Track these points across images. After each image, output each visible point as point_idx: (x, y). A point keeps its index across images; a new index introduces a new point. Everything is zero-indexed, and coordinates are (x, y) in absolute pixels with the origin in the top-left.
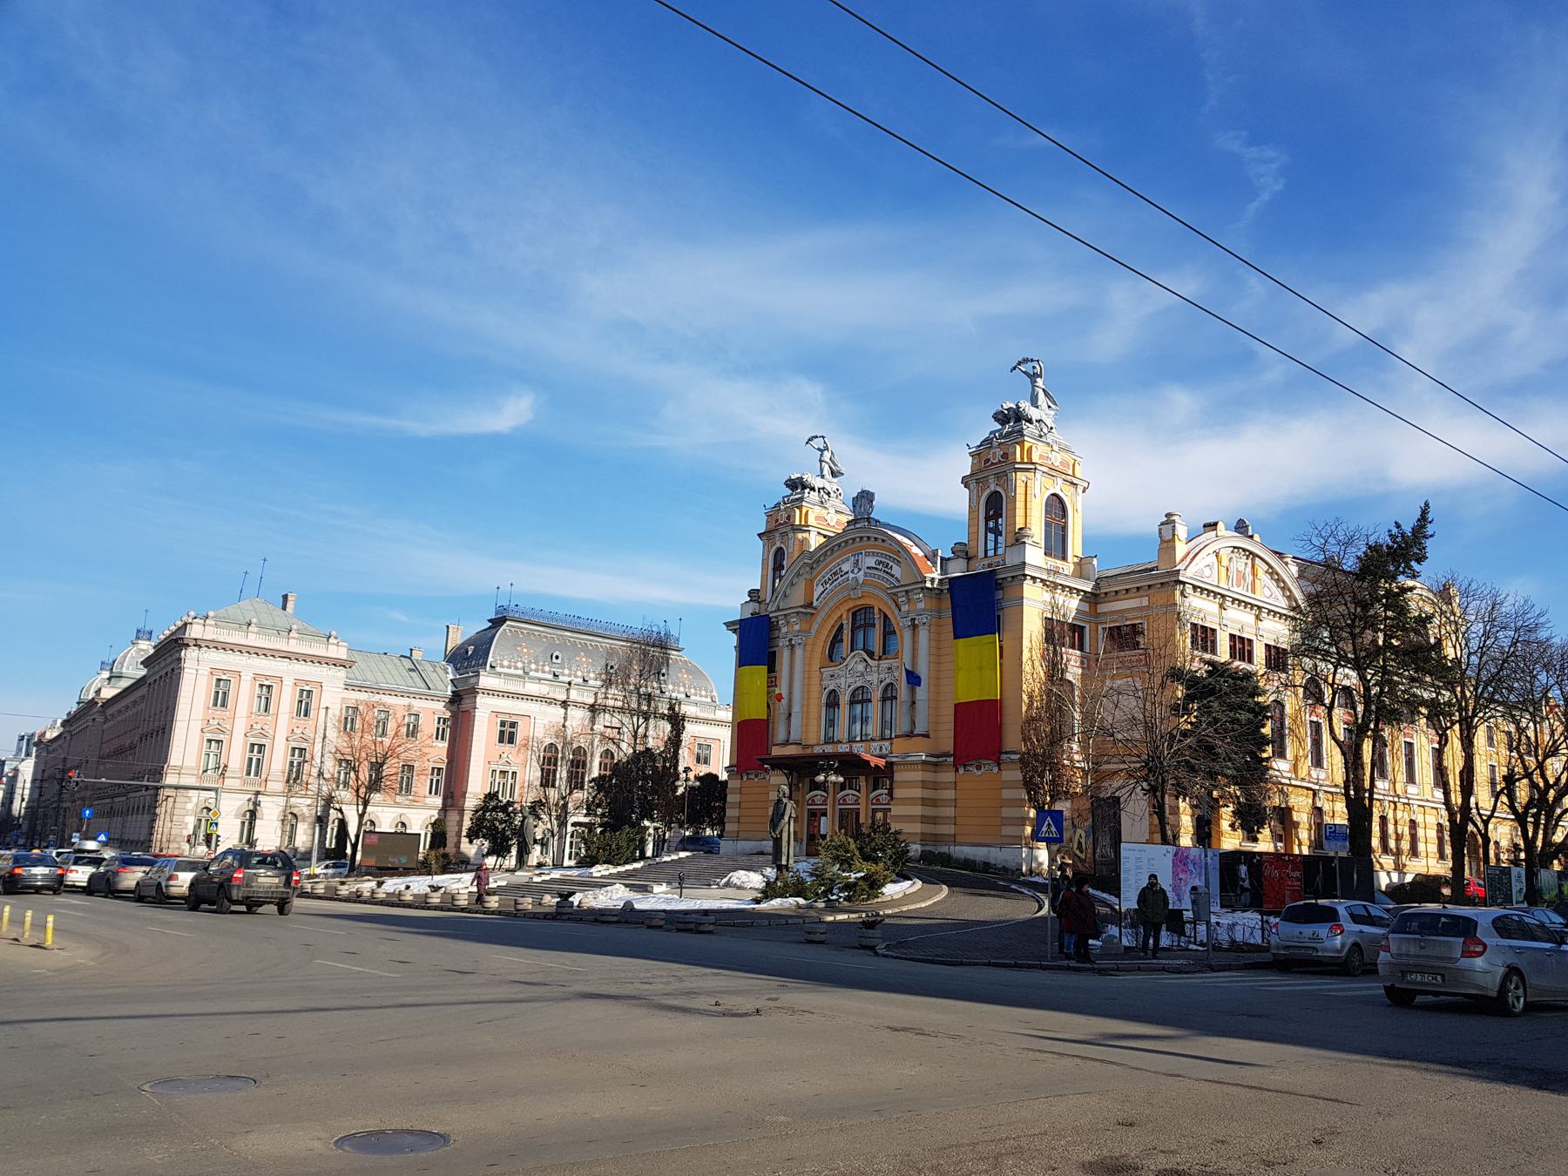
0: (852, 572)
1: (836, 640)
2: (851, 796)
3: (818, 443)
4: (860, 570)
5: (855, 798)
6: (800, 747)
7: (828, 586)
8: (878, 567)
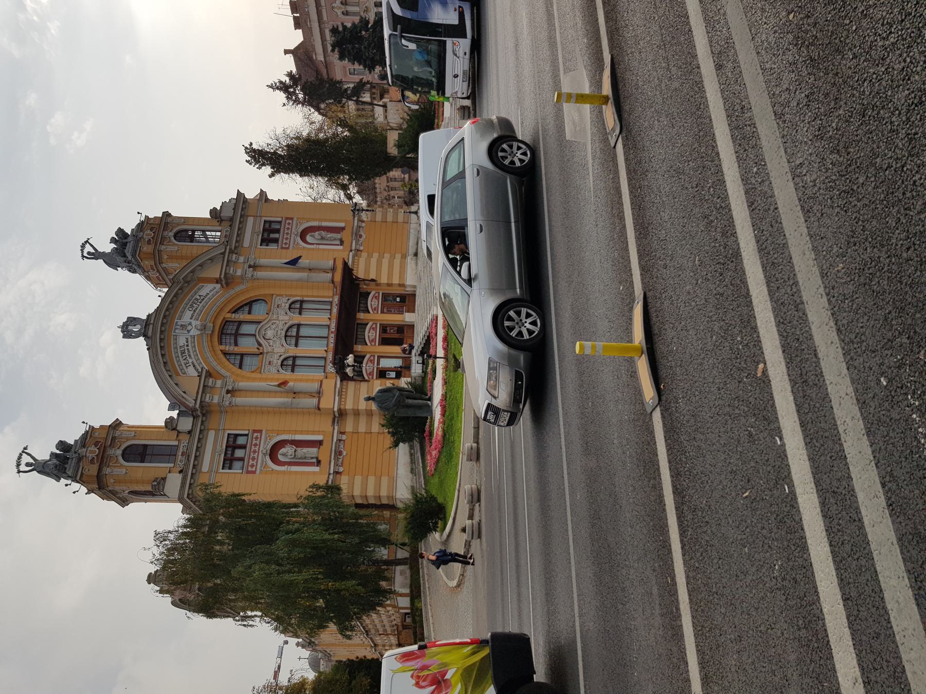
0: (189, 331)
2: (370, 334)
3: (23, 468)
4: (190, 324)
5: (372, 330)
7: (190, 361)
8: (194, 309)
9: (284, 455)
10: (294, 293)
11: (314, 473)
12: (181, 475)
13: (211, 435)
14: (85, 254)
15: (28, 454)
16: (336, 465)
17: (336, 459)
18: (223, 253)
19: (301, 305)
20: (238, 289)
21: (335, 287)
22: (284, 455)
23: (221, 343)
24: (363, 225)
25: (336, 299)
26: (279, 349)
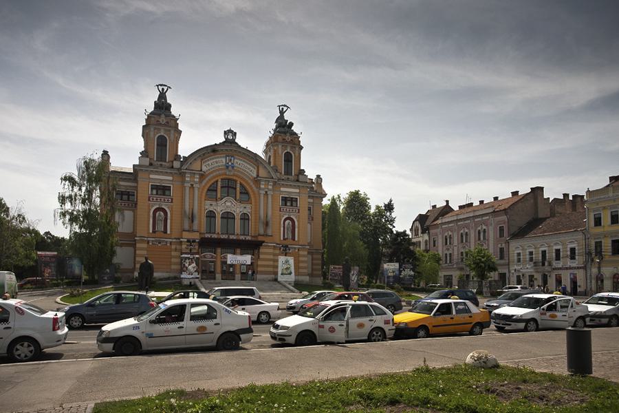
1: (212, 190)
3: (160, 88)
6: (198, 234)
9: (160, 215)
10: (253, 215)
11: (149, 230)
12: (148, 164)
13: (171, 178)
14: (281, 107)
15: (167, 89)
16: (153, 241)
17: (156, 241)
18: (272, 178)
19: (247, 219)
20: (253, 186)
21: (254, 237)
22: (160, 215)
23: (222, 179)
24: (297, 250)
25: (249, 238)
26: (220, 208)
